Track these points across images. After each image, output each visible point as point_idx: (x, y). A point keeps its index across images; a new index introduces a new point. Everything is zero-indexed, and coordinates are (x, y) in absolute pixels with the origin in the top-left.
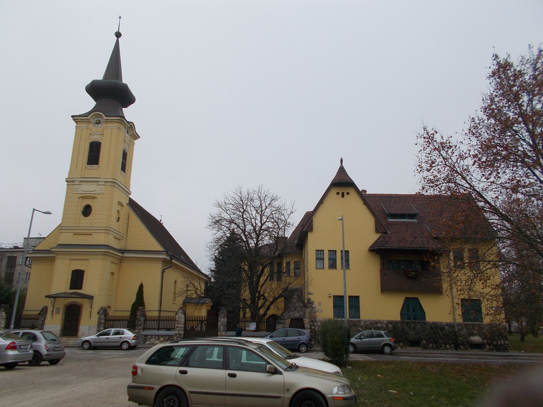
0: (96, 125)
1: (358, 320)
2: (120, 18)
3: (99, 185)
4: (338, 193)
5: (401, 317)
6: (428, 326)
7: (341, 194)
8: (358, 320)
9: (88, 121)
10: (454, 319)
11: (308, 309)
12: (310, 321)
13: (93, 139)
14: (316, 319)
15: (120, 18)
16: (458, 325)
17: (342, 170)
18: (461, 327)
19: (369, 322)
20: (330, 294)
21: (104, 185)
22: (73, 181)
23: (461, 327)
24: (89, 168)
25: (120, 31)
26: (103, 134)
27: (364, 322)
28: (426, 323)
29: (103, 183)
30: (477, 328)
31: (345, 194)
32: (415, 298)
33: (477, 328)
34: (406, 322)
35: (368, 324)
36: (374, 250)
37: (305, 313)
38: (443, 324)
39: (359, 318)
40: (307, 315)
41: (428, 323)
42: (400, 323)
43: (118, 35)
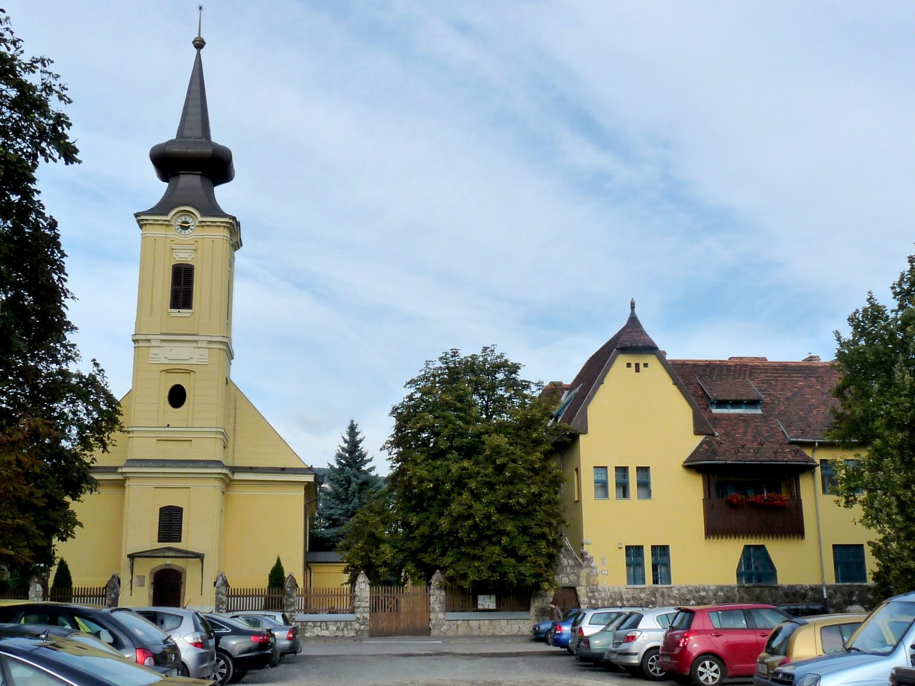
0: (178, 229)
1: (668, 586)
2: (201, 8)
3: (199, 348)
4: (629, 365)
6: (780, 592)
7: (633, 366)
9: (167, 223)
10: (823, 578)
11: (584, 570)
12: (588, 590)
13: (177, 259)
14: (599, 587)
15: (201, 8)
16: (828, 588)
17: (633, 321)
20: (621, 544)
21: (206, 348)
22: (149, 340)
23: (832, 592)
24: (173, 315)
25: (201, 36)
26: (195, 250)
27: (679, 590)
28: (777, 588)
29: (205, 345)
30: (857, 592)
31: (641, 366)
35: (685, 593)
36: (692, 466)
37: (578, 576)
40: (583, 581)
41: (782, 588)
42: (736, 589)
43: (199, 44)
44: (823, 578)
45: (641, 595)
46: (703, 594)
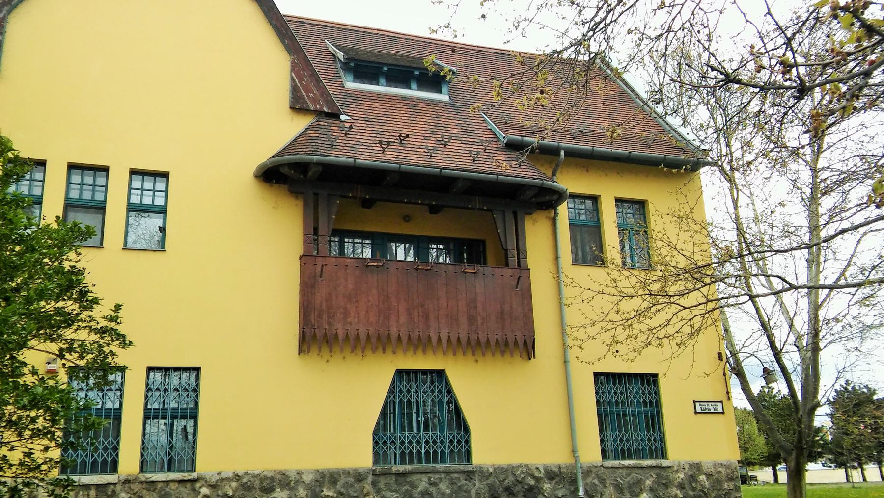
5: (376, 454)
6: (478, 485)
8: (187, 476)
10: (574, 451)
18: (596, 482)
19: (234, 484)
23: (596, 482)
27: (213, 487)
32: (432, 372)
33: (648, 482)
38: (536, 474)
39: (193, 469)
41: (482, 473)
42: (370, 478)
44: (574, 451)
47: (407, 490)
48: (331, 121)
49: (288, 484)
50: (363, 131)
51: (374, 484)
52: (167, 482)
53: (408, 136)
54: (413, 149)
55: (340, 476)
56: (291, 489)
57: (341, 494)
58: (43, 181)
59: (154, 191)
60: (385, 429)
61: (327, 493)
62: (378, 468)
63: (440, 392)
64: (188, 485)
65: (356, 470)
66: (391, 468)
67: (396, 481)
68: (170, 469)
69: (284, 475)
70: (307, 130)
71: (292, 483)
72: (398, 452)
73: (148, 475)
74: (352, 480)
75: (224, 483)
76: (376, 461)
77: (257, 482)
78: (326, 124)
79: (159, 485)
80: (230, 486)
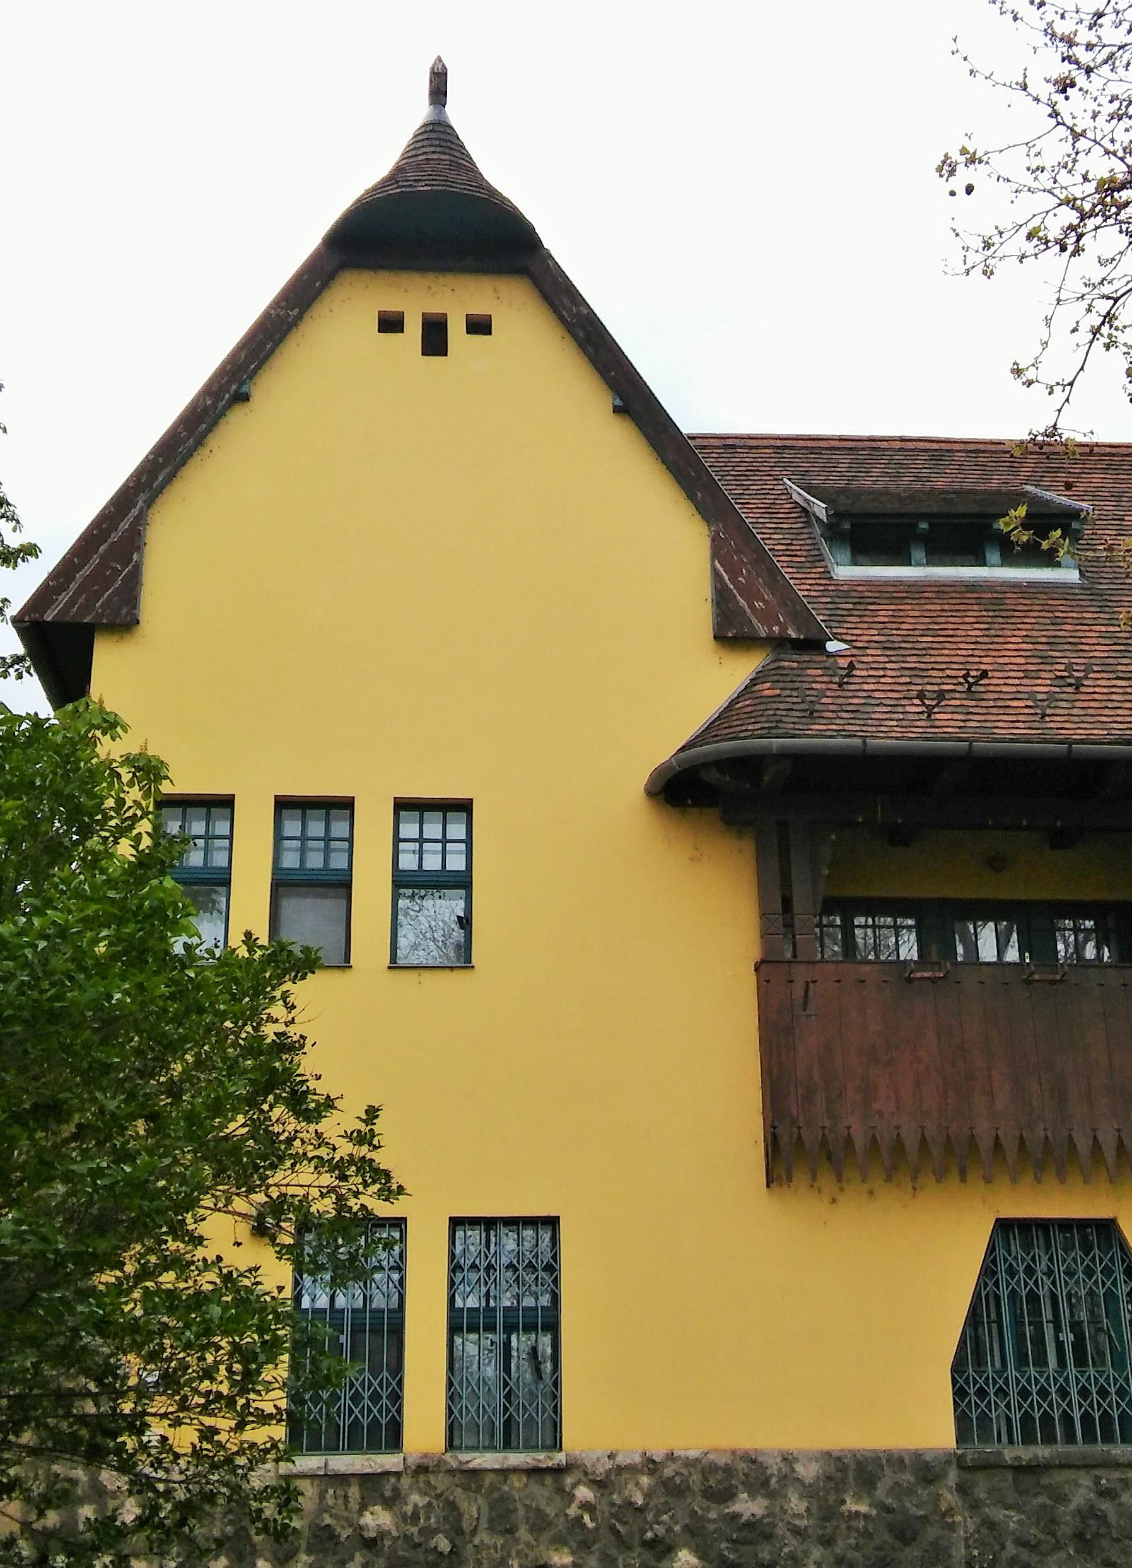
8: (542, 1458)
19: (645, 1480)
27: (601, 1484)
32: (1083, 1224)
34: (1020, 1469)
39: (556, 1444)
42: (953, 1476)
45: (368, 1519)
46: (748, 1506)
47: (1044, 1507)
48: (807, 658)
49: (766, 1483)
50: (881, 673)
51: (962, 1489)
52: (504, 1473)
53: (984, 674)
54: (1000, 703)
55: (881, 1467)
56: (772, 1495)
57: (889, 1510)
58: (231, 838)
59: (444, 841)
60: (979, 1361)
61: (854, 1508)
62: (976, 1450)
63: (1107, 1272)
64: (549, 1480)
65: (917, 1455)
66: (1000, 1454)
67: (1016, 1483)
68: (508, 1445)
69: (754, 1461)
70: (753, 682)
71: (774, 1481)
72: (1016, 1416)
73: (464, 1456)
74: (908, 1477)
75: (625, 1476)
76: (962, 1435)
77: (696, 1477)
78: (795, 665)
79: (488, 1479)
80: (637, 1484)
